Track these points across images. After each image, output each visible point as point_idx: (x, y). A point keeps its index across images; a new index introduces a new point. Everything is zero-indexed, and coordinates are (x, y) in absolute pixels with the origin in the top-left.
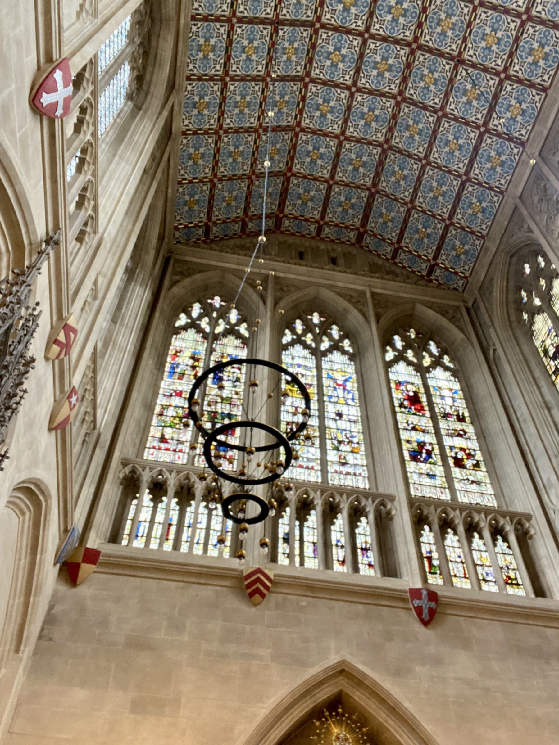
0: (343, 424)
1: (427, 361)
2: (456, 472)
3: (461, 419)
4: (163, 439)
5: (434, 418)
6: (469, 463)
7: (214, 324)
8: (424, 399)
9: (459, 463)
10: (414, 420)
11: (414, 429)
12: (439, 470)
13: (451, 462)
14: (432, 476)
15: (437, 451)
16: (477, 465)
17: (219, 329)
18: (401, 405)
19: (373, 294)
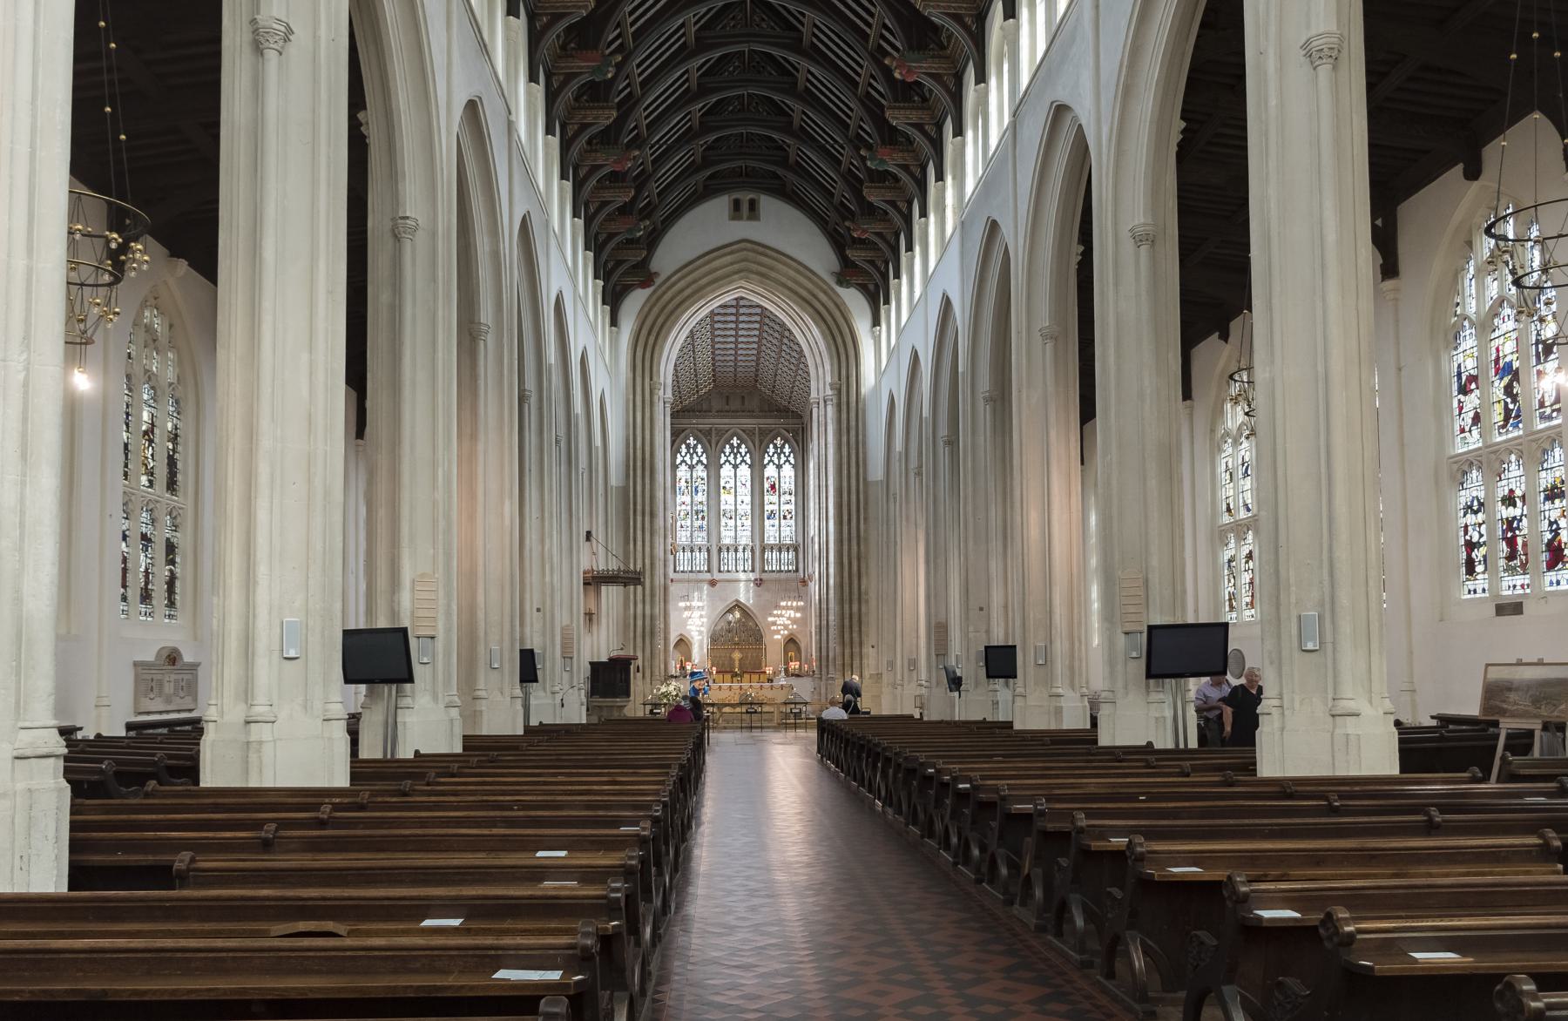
0: (744, 506)
1: (782, 462)
2: (783, 521)
3: (790, 494)
4: (682, 527)
5: (780, 496)
6: (788, 517)
7: (692, 458)
8: (777, 486)
9: (785, 518)
10: (771, 497)
11: (771, 503)
12: (777, 522)
13: (782, 517)
14: (773, 526)
15: (778, 514)
16: (791, 518)
17: (694, 462)
18: (768, 491)
19: (759, 428)
